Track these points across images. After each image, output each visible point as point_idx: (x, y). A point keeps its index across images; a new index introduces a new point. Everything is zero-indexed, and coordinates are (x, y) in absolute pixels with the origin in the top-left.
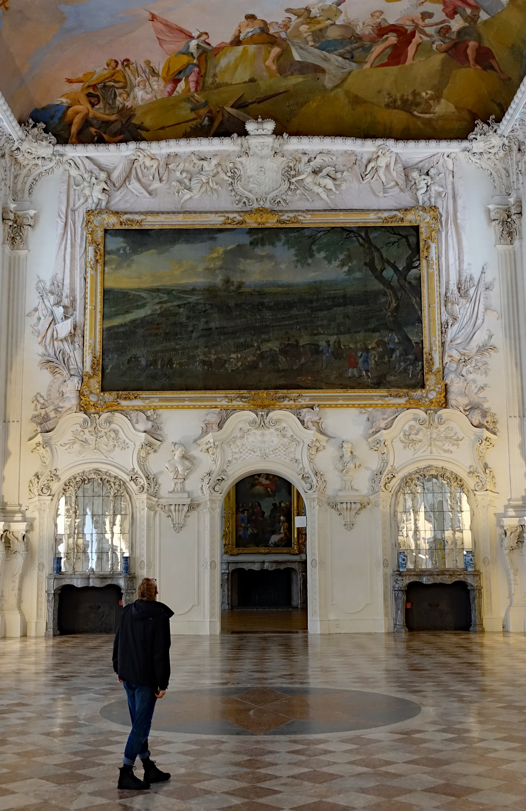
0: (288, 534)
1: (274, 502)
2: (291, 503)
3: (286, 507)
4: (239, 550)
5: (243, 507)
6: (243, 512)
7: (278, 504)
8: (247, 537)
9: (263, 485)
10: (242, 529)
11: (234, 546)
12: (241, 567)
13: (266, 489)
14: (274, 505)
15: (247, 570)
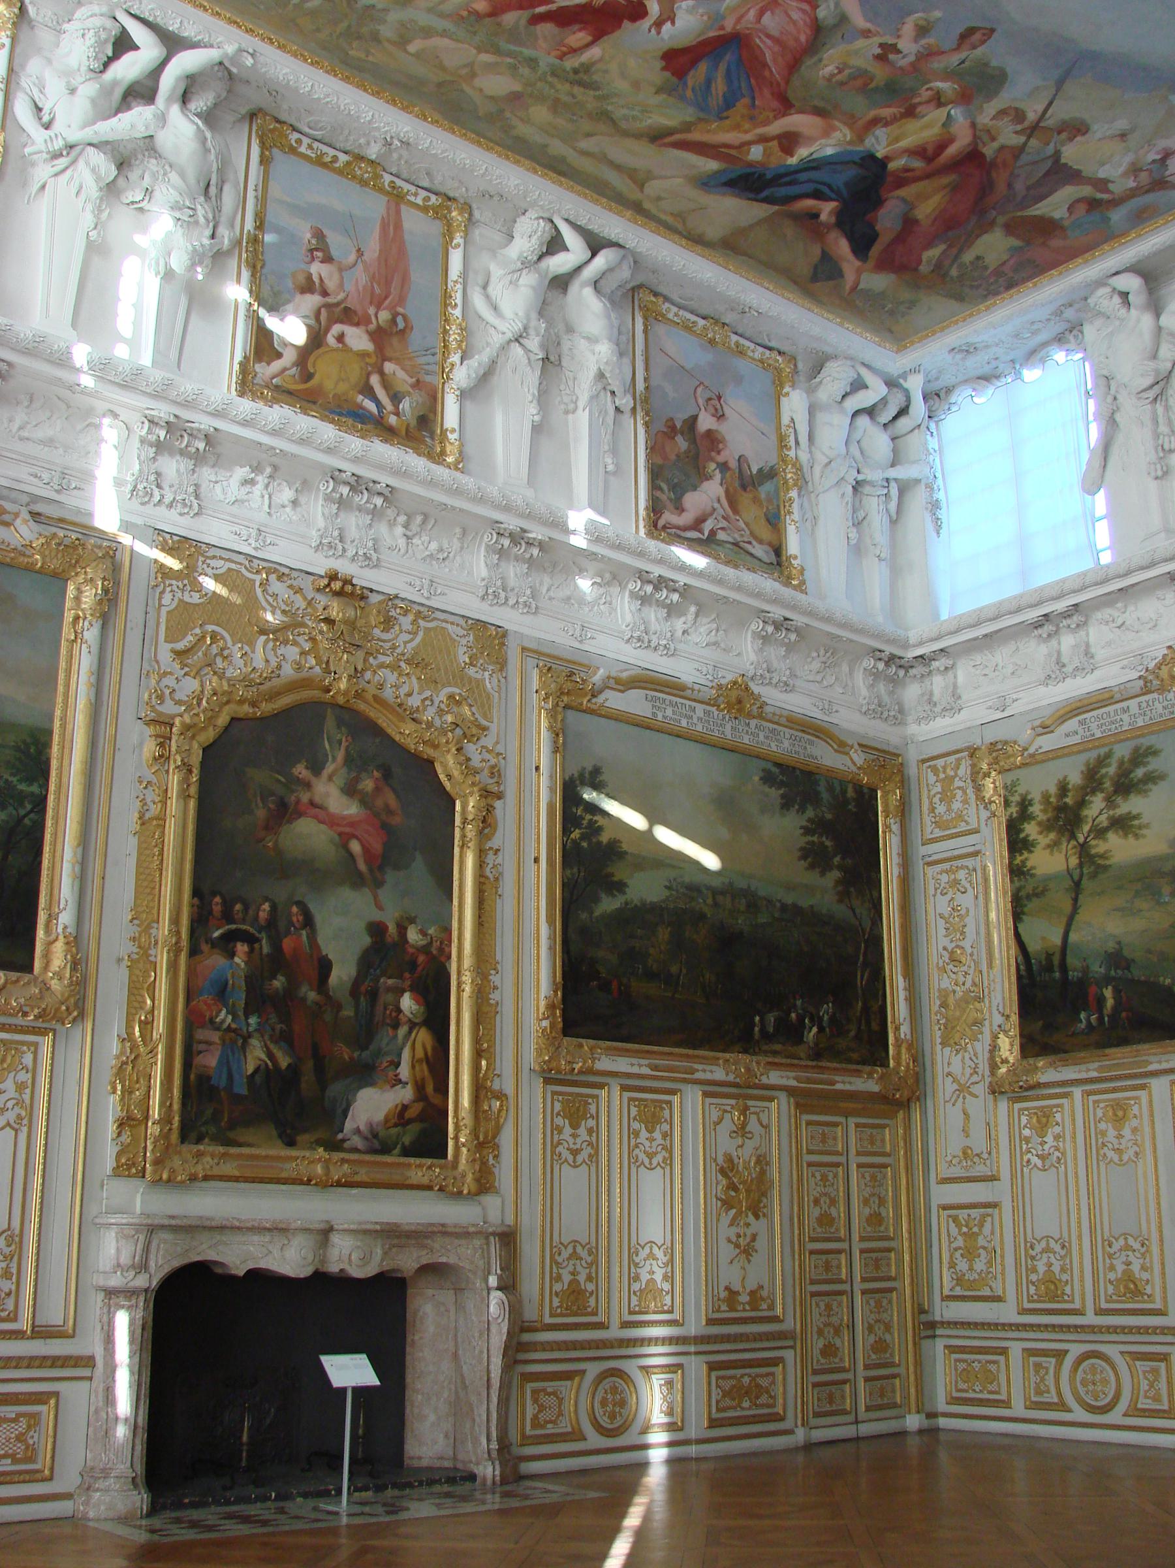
0: (430, 1088)
1: (377, 916)
2: (448, 931)
3: (425, 950)
4: (200, 1154)
5: (228, 917)
6: (227, 944)
7: (392, 929)
8: (241, 1089)
9: (331, 821)
10: (215, 1037)
11: (175, 1137)
12: (211, 1255)
13: (344, 840)
14: (377, 930)
15: (241, 1273)
